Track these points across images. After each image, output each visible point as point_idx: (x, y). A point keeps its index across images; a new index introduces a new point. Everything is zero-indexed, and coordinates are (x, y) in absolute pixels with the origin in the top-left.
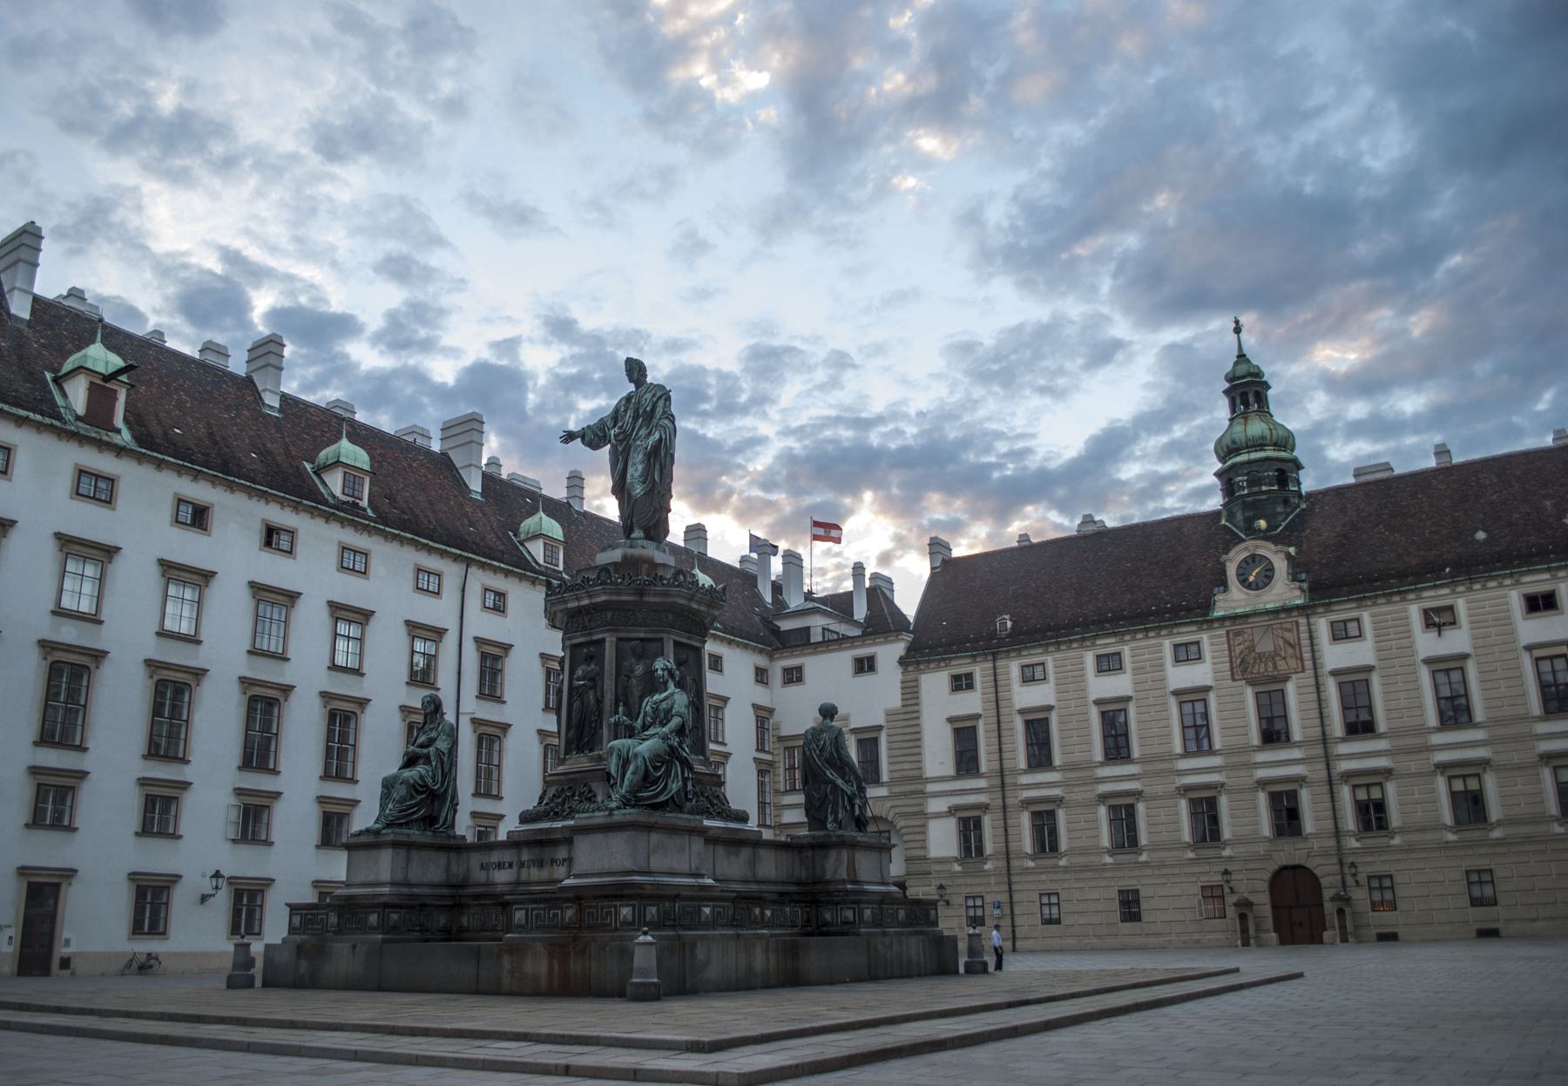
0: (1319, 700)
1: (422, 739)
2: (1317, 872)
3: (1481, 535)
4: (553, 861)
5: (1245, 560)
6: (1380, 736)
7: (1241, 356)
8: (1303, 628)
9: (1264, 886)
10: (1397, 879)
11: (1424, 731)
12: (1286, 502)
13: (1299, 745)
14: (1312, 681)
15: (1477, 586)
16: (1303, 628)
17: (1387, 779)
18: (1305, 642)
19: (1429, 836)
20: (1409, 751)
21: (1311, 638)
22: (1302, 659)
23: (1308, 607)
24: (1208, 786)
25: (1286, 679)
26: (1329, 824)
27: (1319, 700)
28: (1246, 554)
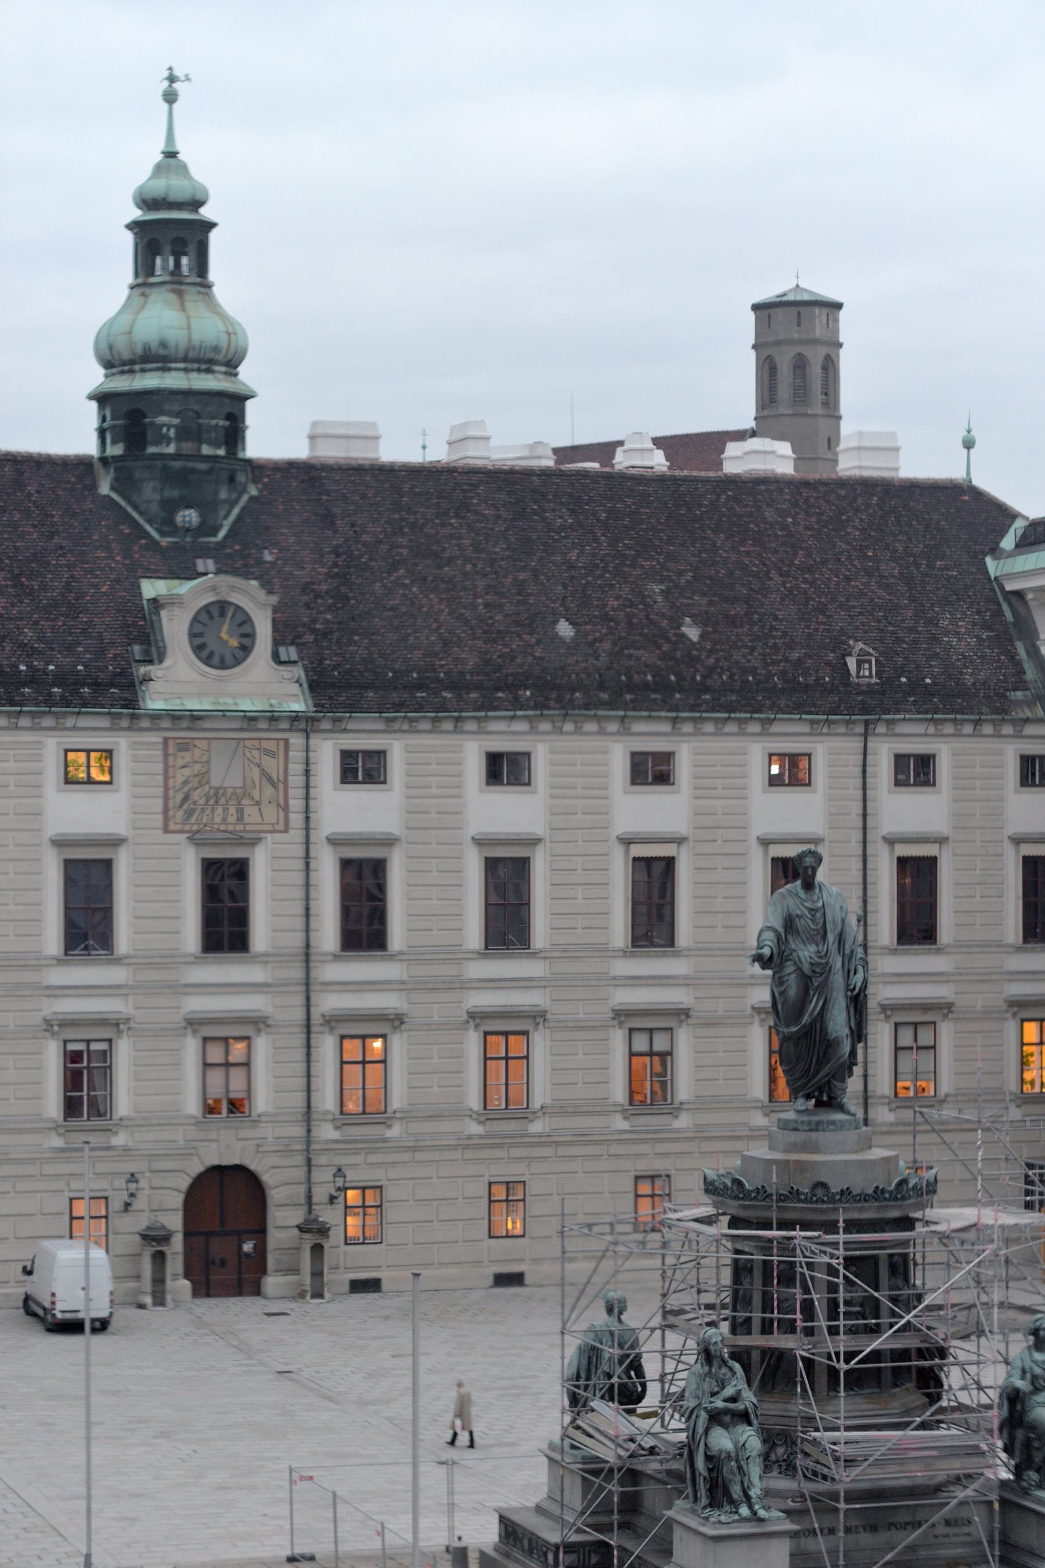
0: (307, 885)
1: (729, 1391)
2: (267, 1178)
3: (565, 629)
4: (892, 1525)
5: (206, 609)
6: (393, 957)
7: (171, 155)
8: (296, 755)
9: (177, 1200)
10: (390, 1193)
11: (455, 954)
12: (232, 479)
13: (264, 959)
14: (300, 851)
15: (569, 727)
16: (296, 755)
17: (395, 1028)
18: (296, 780)
19: (445, 1126)
20: (432, 986)
21: (307, 772)
22: (286, 809)
23: (313, 720)
24: (103, 1022)
25: (254, 842)
26: (298, 1100)
27: (307, 885)
28: (210, 598)
